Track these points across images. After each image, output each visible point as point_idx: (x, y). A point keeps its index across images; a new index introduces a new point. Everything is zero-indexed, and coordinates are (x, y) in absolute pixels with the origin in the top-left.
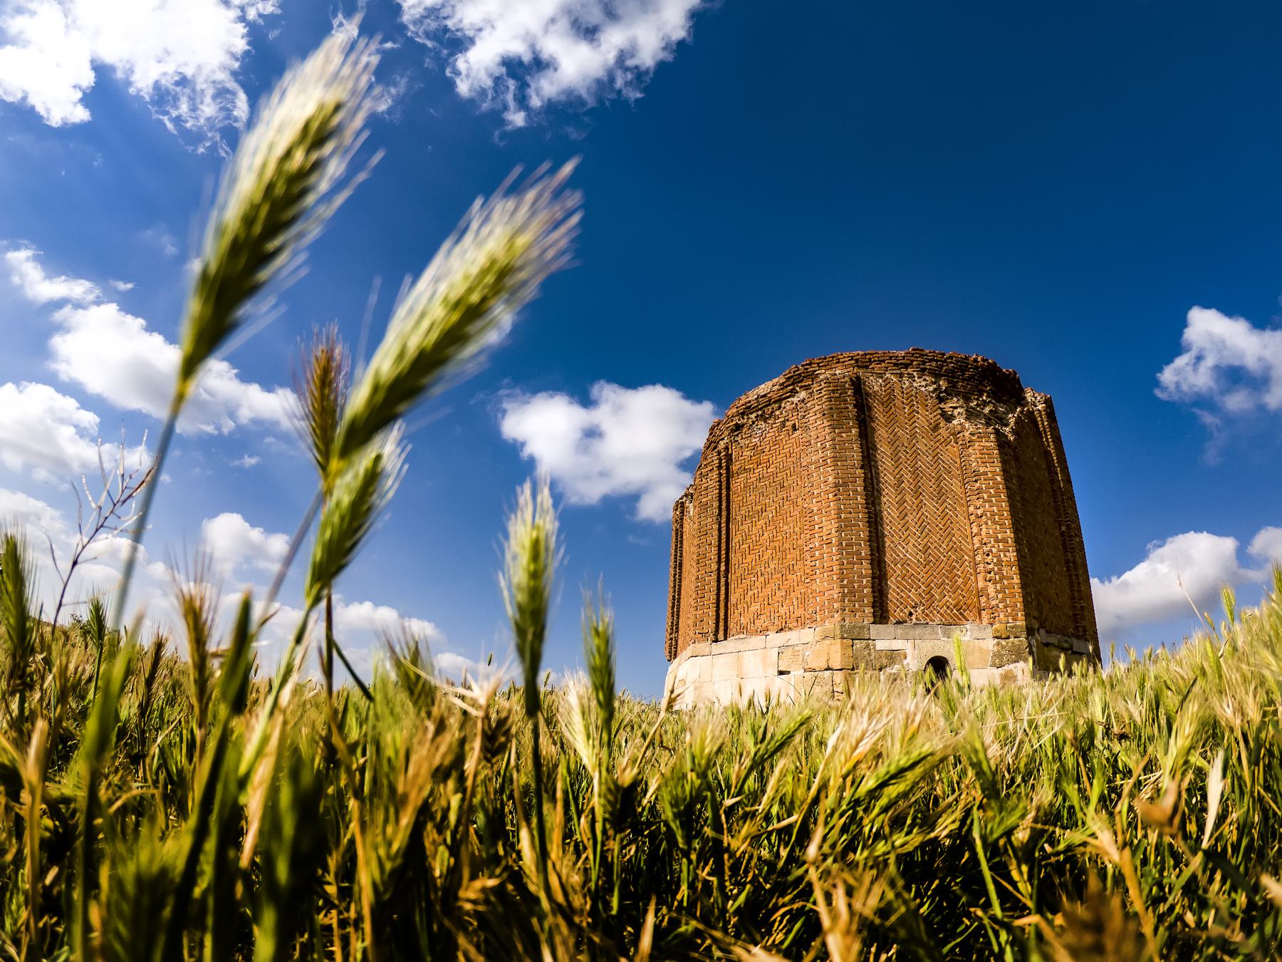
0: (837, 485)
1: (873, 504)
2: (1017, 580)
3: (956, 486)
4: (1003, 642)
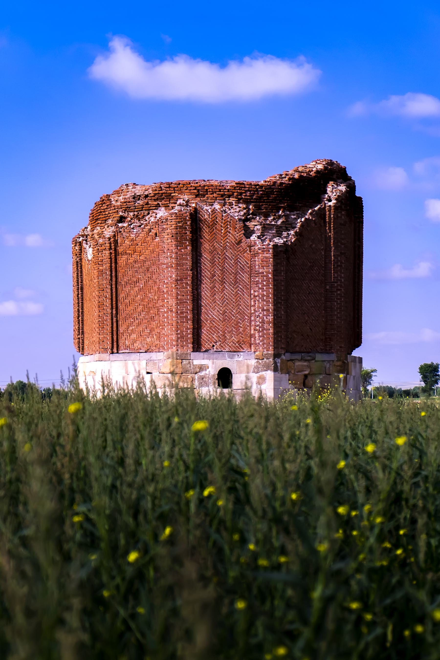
0: (177, 280)
1: (197, 290)
2: (271, 331)
3: (245, 277)
4: (260, 361)
